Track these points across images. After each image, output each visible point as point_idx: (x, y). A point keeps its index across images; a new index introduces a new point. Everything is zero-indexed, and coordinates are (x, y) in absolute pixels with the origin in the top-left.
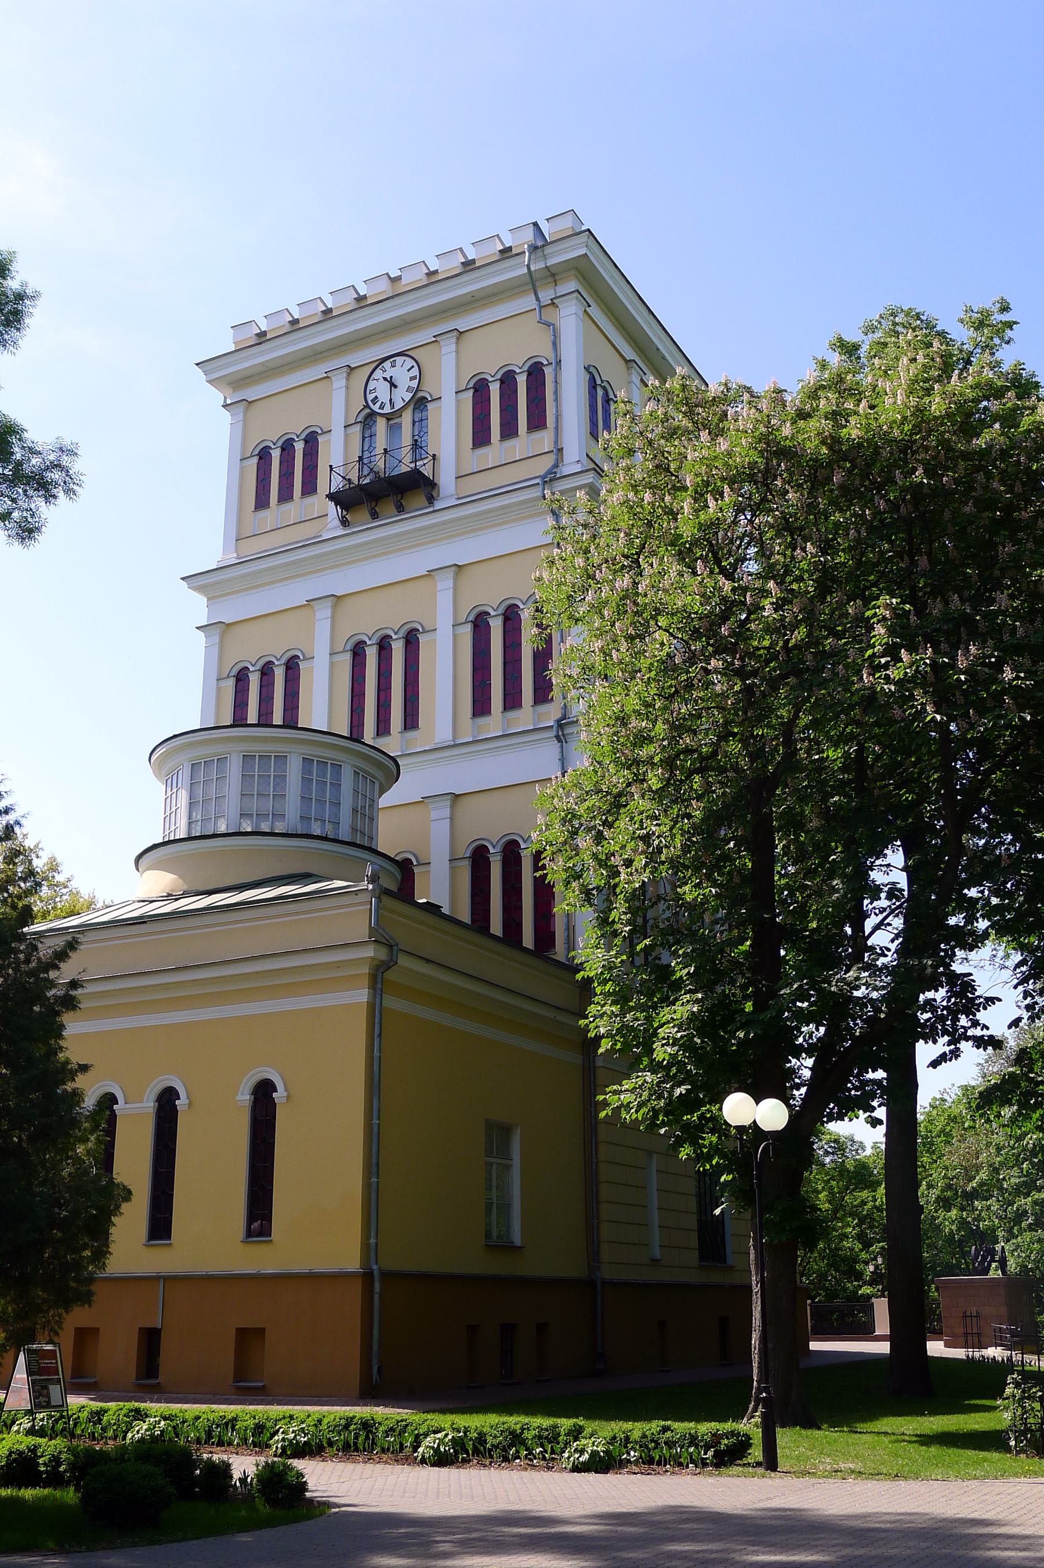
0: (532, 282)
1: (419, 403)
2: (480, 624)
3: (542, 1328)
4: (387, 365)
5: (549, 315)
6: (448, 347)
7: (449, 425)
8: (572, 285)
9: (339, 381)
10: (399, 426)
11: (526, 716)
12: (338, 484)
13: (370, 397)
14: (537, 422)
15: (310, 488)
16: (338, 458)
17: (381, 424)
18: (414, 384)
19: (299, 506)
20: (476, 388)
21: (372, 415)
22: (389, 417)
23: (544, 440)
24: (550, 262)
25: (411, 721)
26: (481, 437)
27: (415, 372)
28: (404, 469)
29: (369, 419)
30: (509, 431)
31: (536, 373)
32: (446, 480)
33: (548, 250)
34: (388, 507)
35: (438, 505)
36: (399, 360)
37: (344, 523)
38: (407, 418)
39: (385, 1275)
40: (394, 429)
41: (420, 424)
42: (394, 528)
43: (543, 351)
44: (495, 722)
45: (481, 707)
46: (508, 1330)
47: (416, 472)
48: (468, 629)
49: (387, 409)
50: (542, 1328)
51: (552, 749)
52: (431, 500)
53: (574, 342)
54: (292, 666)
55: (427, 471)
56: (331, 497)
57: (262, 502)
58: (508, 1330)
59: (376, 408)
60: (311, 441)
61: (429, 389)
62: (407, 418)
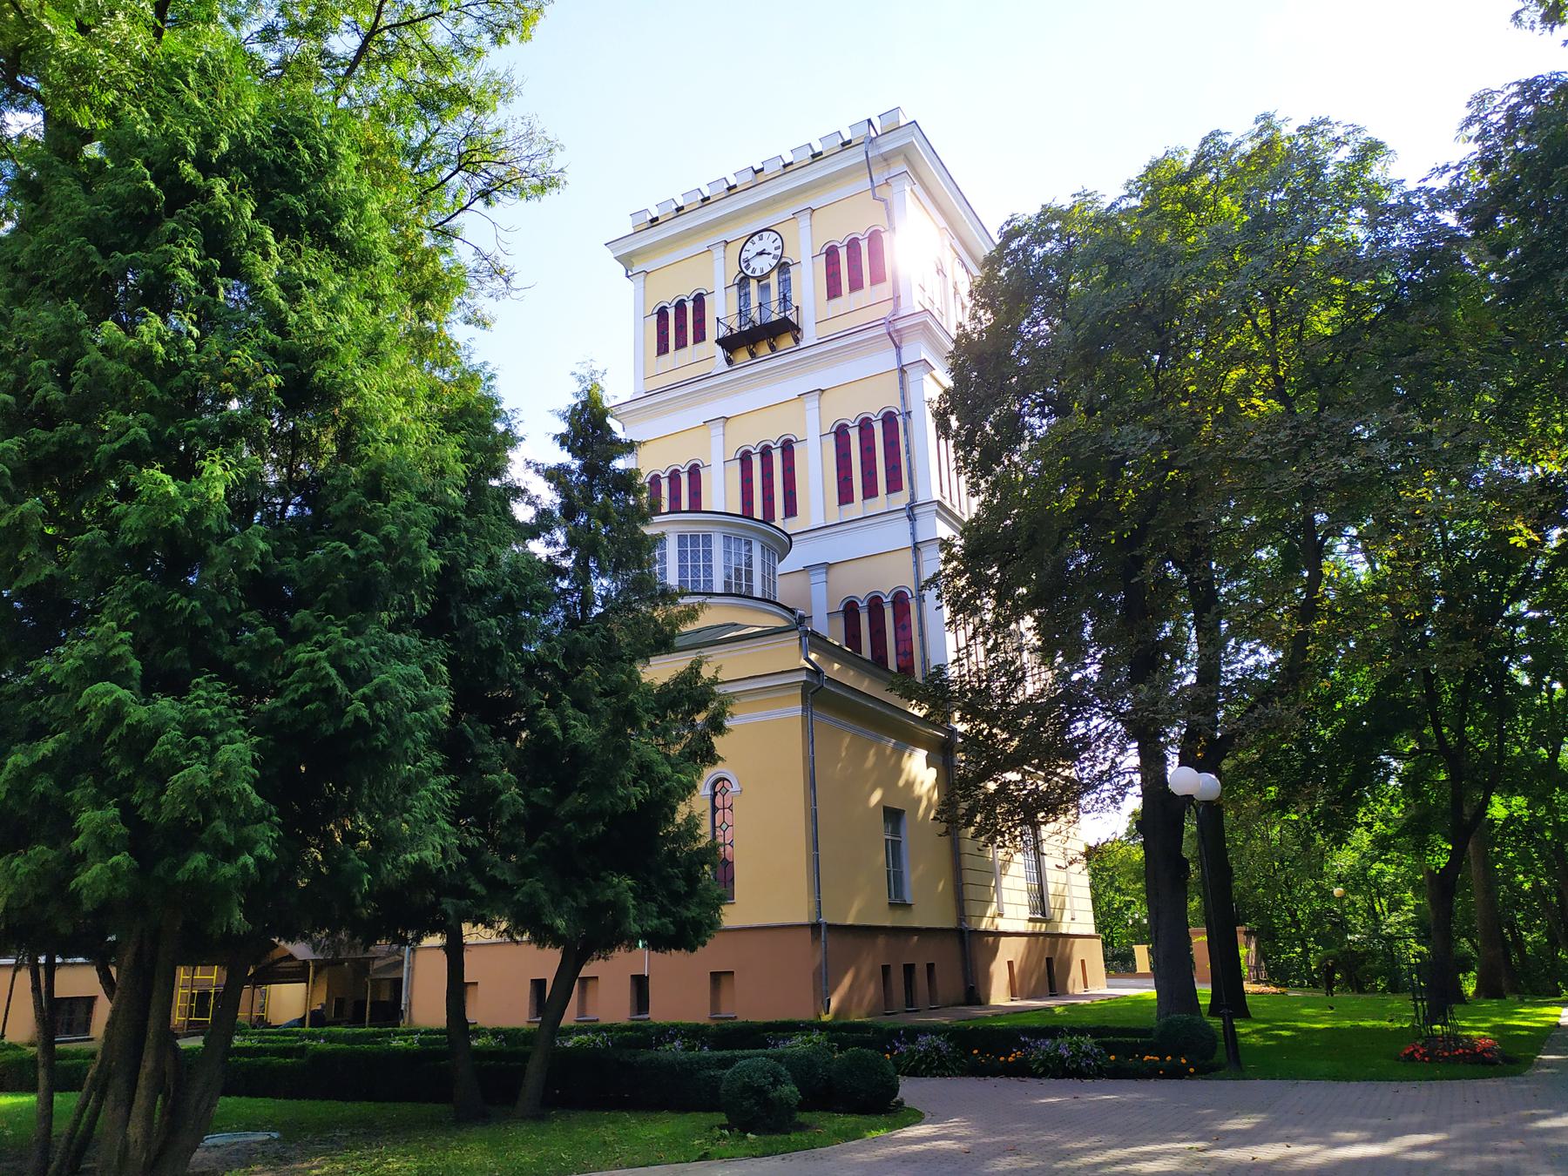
1: (783, 267)
2: (841, 433)
3: (930, 967)
4: (756, 238)
5: (883, 192)
6: (804, 221)
7: (808, 283)
9: (718, 252)
10: (768, 286)
11: (882, 502)
12: (723, 332)
15: (700, 336)
16: (722, 312)
17: (753, 283)
18: (779, 252)
19: (692, 351)
20: (827, 253)
21: (747, 277)
24: (883, 150)
25: (791, 510)
26: (833, 291)
27: (779, 242)
28: (775, 317)
29: (743, 282)
33: (880, 141)
35: (802, 345)
36: (765, 234)
37: (729, 362)
38: (774, 277)
39: (829, 927)
40: (765, 289)
41: (785, 283)
42: (767, 362)
44: (858, 507)
45: (845, 497)
46: (909, 969)
47: (786, 318)
48: (831, 439)
49: (758, 274)
50: (930, 967)
52: (797, 341)
54: (788, 448)
55: (793, 318)
56: (719, 342)
57: (663, 349)
58: (909, 969)
59: (749, 273)
60: (699, 300)
61: (789, 256)
62: (774, 277)
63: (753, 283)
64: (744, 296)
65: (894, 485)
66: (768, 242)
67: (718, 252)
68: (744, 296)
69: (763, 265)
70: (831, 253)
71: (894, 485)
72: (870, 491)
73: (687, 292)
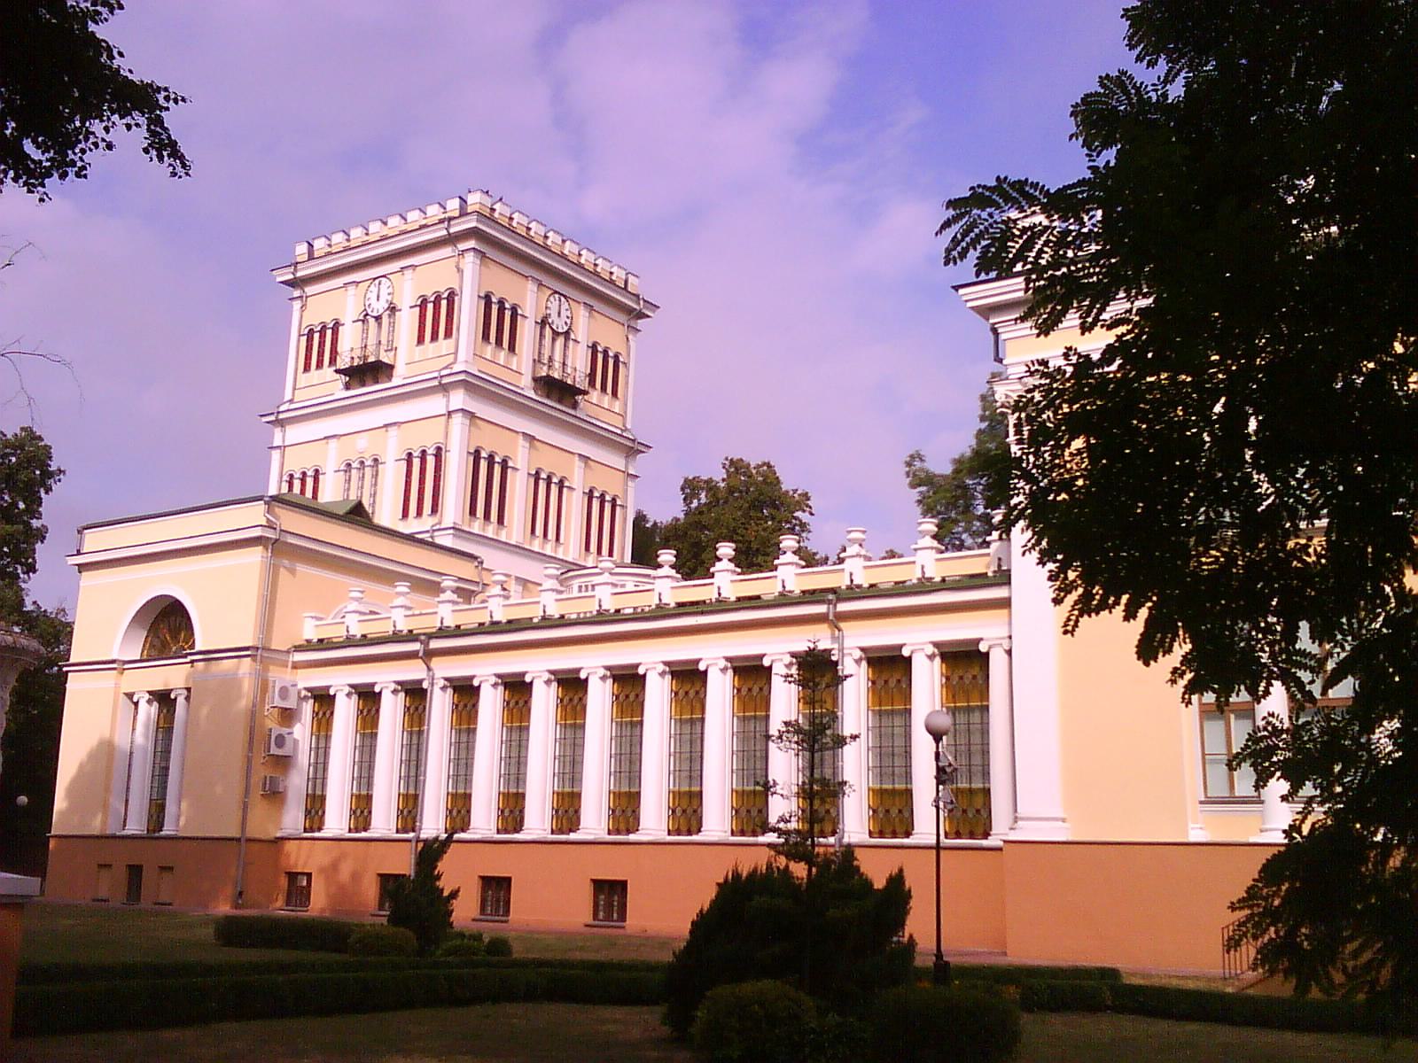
1: (393, 309)
6: (408, 273)
12: (343, 363)
13: (367, 304)
15: (333, 361)
16: (350, 346)
22: (378, 318)
30: (434, 337)
34: (369, 379)
35: (396, 381)
36: (383, 280)
37: (347, 387)
41: (392, 325)
52: (390, 377)
59: (369, 311)
62: (385, 320)
63: (372, 321)
67: (351, 289)
69: (379, 307)
70: (423, 306)
73: (329, 320)
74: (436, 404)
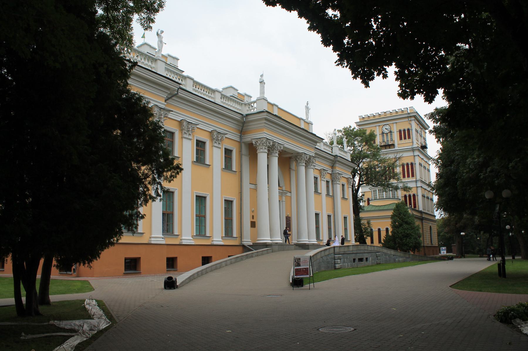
0: (408, 117)
6: (395, 125)
7: (396, 136)
8: (413, 118)
9: (378, 127)
14: (409, 138)
17: (385, 135)
23: (410, 140)
26: (401, 139)
29: (383, 133)
31: (408, 130)
32: (396, 144)
35: (396, 148)
41: (391, 135)
43: (409, 127)
51: (415, 183)
53: (414, 126)
62: (389, 134)
63: (385, 135)
64: (383, 136)
65: (413, 176)
66: (387, 127)
67: (378, 127)
68: (383, 136)
69: (386, 131)
71: (413, 176)
72: (408, 176)
74: (411, 154)
